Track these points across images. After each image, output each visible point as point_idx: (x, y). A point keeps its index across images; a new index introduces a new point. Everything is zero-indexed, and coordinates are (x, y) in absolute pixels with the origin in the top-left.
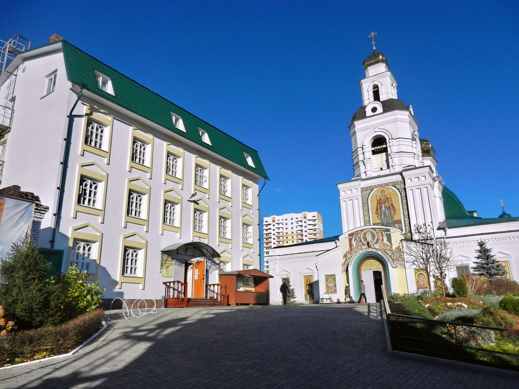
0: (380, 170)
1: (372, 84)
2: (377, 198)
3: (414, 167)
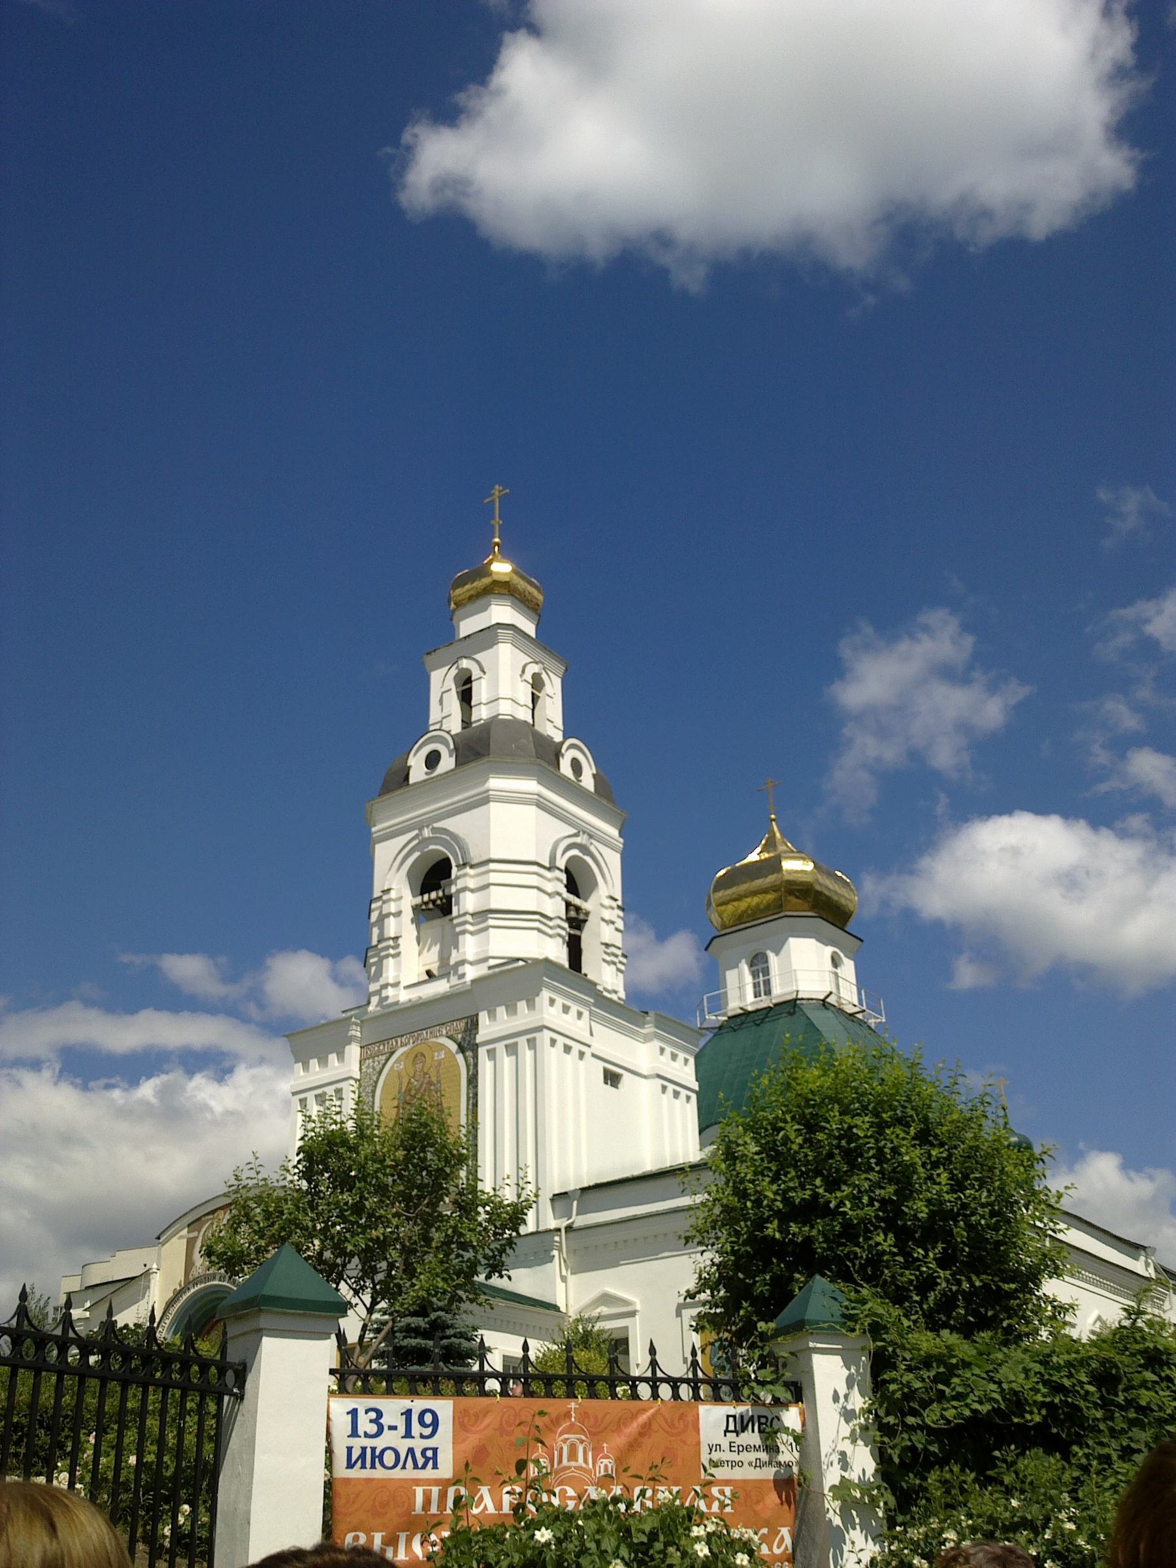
0: (427, 978)
1: (454, 671)
2: (401, 1084)
3: (521, 963)
